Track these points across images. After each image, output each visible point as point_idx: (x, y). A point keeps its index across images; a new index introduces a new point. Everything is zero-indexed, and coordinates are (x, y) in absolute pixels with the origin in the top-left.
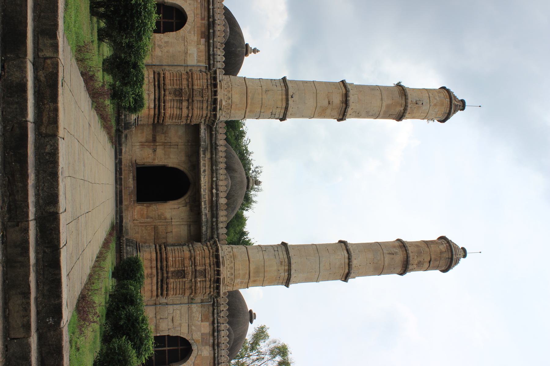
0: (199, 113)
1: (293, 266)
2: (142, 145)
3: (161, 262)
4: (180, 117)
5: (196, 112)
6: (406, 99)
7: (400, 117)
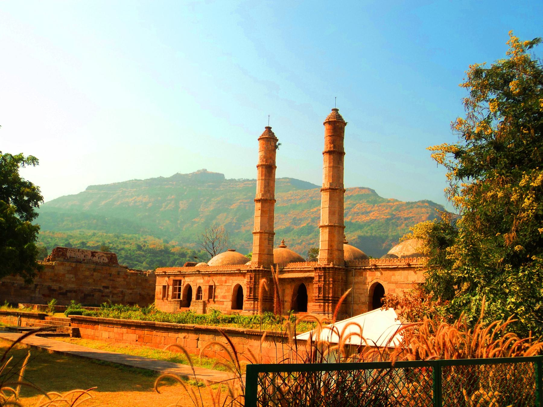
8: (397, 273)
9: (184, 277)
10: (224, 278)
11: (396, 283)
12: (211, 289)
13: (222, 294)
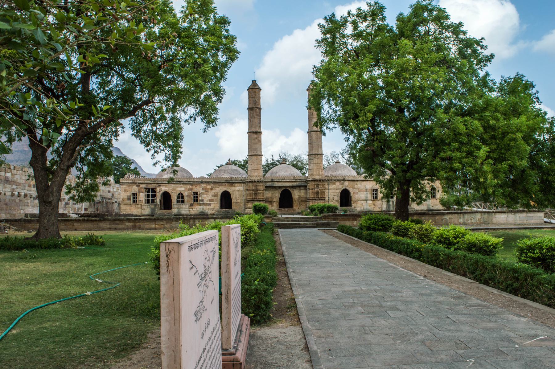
0: (261, 187)
1: (316, 153)
2: (272, 206)
3: (314, 199)
4: (263, 193)
5: (261, 188)
6: (254, 108)
7: (260, 109)
8: (359, 183)
9: (160, 186)
10: (209, 187)
11: (358, 189)
12: (196, 196)
13: (210, 198)
